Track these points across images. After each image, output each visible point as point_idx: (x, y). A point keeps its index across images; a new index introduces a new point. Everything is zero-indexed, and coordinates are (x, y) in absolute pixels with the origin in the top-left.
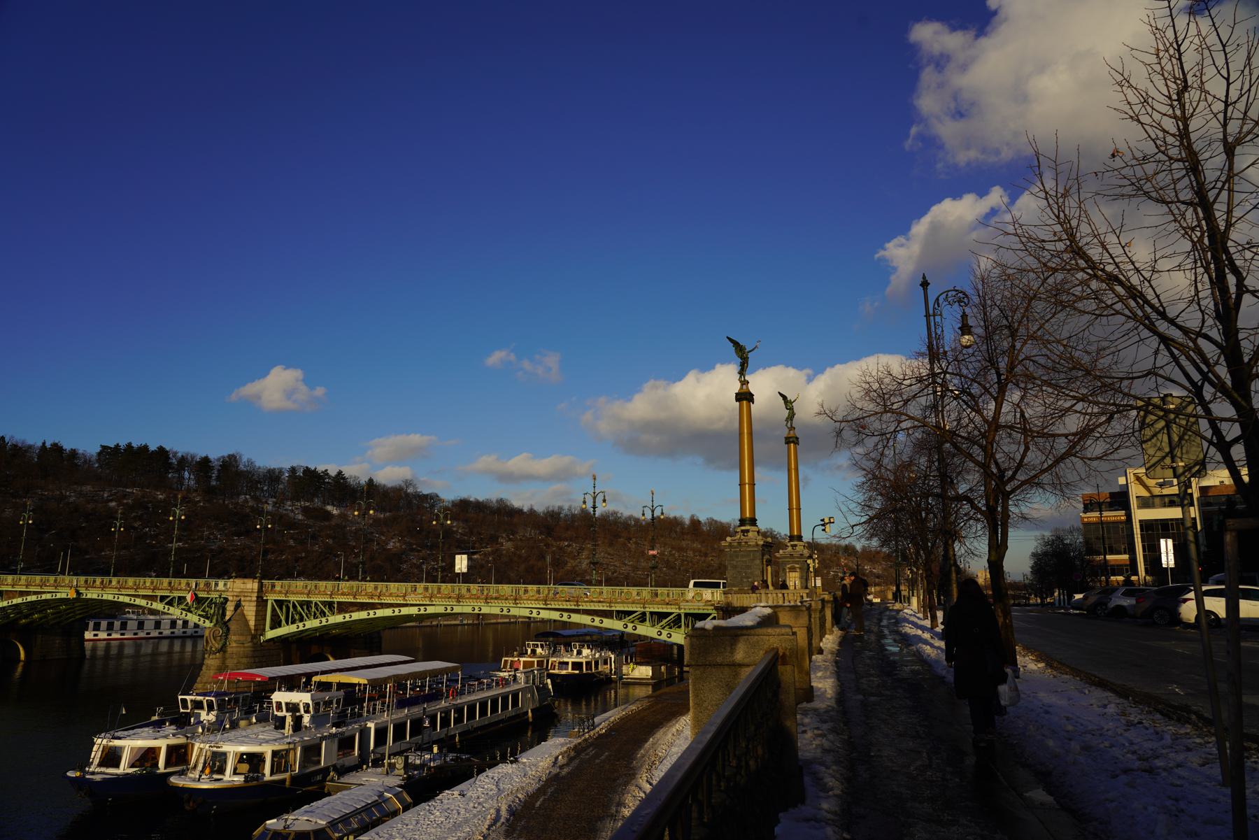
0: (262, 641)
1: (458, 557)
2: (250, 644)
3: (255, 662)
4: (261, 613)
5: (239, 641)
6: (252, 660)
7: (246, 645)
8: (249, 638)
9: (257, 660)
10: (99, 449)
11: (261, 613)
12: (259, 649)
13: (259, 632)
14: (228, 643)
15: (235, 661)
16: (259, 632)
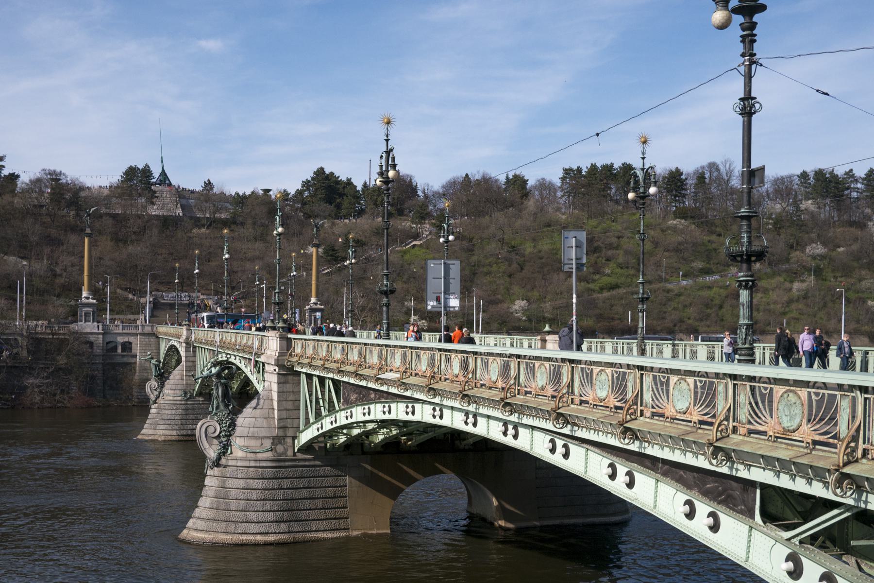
0: (296, 450)
1: (431, 264)
2: (269, 455)
3: (281, 489)
4: (291, 397)
5: (247, 447)
6: (274, 483)
7: (260, 456)
8: (268, 444)
9: (285, 483)
10: (561, 175)
11: (291, 397)
12: (287, 464)
13: (290, 433)
14: (229, 452)
15: (241, 483)
16: (290, 433)
